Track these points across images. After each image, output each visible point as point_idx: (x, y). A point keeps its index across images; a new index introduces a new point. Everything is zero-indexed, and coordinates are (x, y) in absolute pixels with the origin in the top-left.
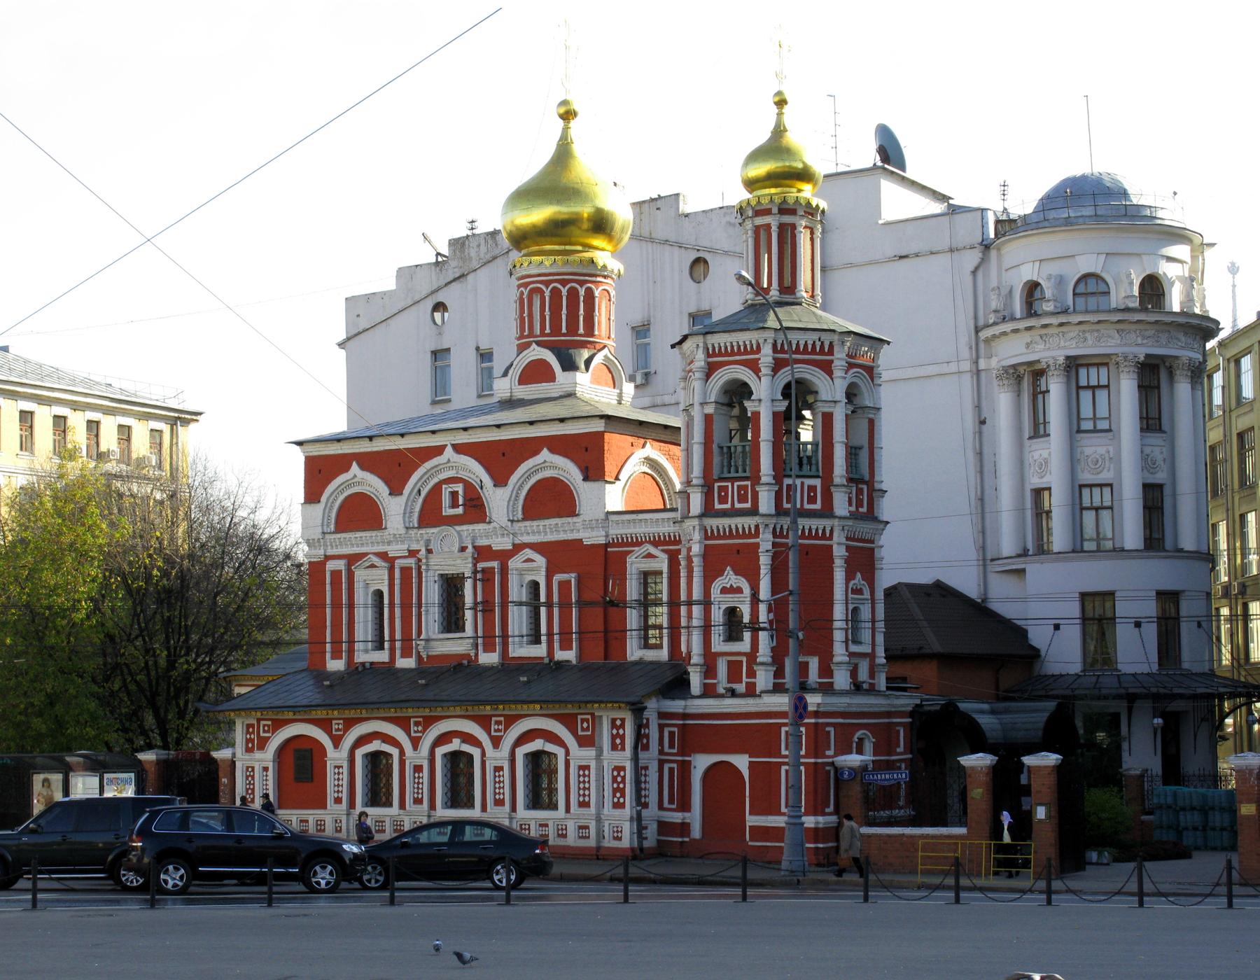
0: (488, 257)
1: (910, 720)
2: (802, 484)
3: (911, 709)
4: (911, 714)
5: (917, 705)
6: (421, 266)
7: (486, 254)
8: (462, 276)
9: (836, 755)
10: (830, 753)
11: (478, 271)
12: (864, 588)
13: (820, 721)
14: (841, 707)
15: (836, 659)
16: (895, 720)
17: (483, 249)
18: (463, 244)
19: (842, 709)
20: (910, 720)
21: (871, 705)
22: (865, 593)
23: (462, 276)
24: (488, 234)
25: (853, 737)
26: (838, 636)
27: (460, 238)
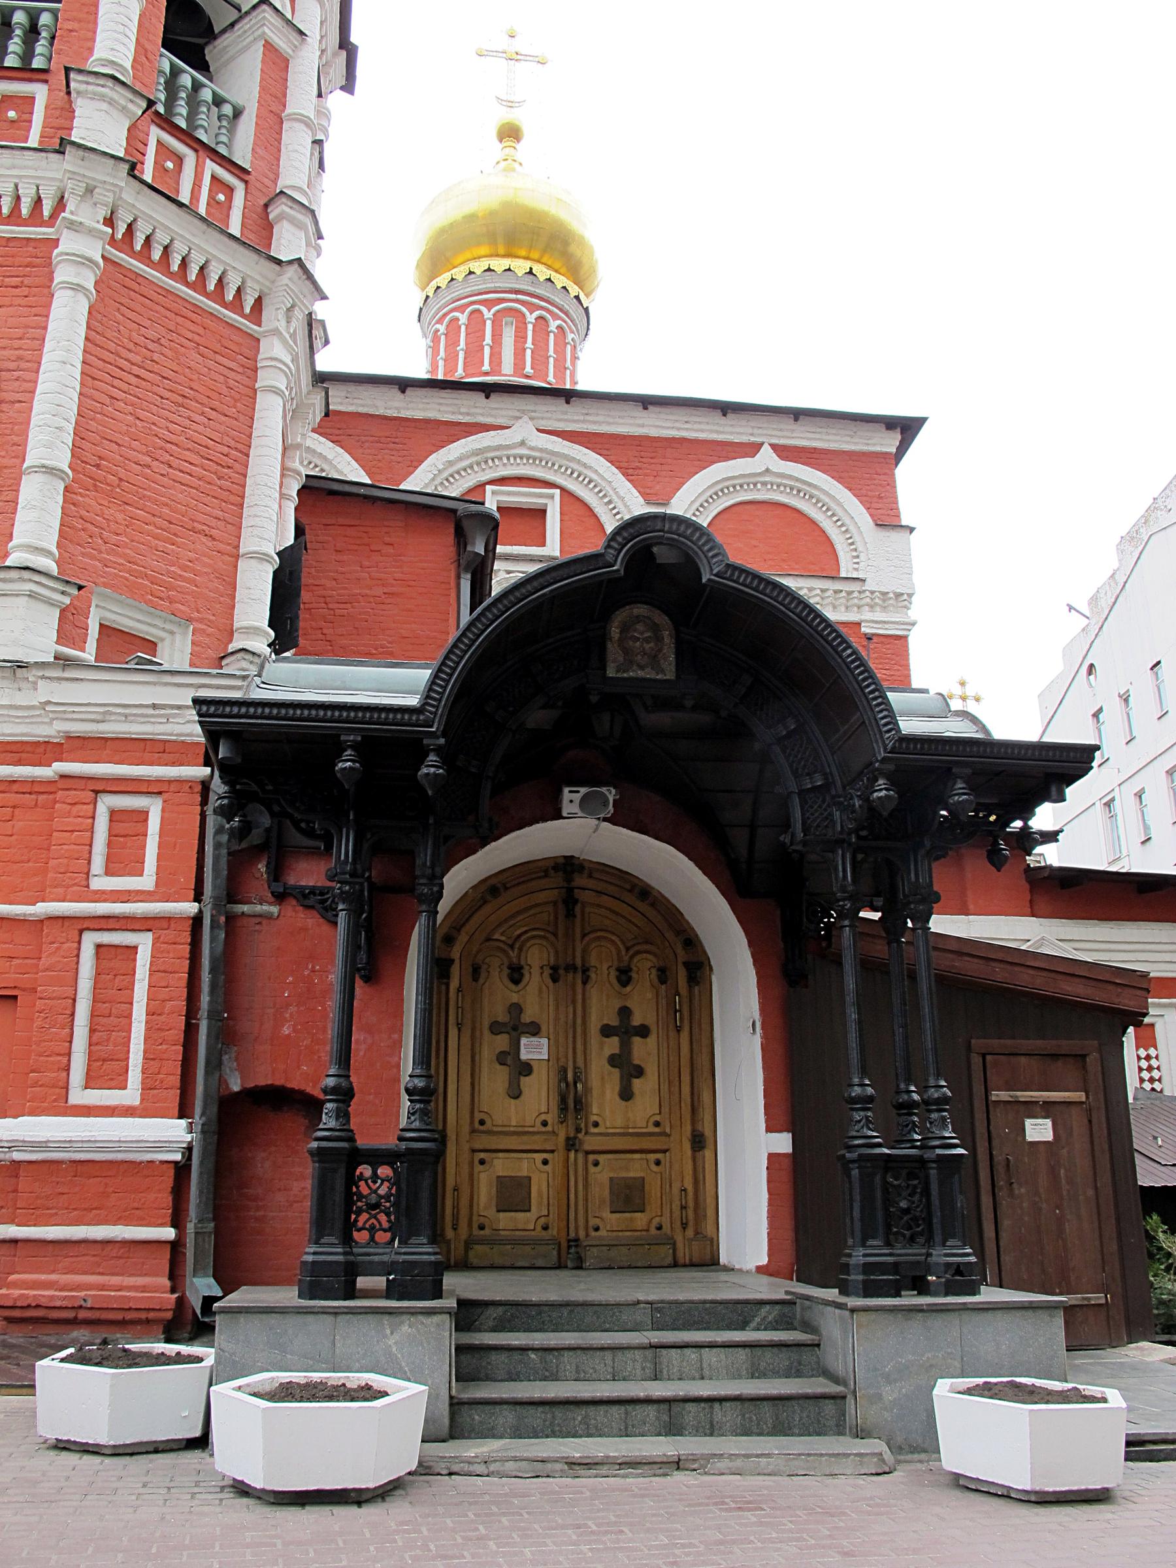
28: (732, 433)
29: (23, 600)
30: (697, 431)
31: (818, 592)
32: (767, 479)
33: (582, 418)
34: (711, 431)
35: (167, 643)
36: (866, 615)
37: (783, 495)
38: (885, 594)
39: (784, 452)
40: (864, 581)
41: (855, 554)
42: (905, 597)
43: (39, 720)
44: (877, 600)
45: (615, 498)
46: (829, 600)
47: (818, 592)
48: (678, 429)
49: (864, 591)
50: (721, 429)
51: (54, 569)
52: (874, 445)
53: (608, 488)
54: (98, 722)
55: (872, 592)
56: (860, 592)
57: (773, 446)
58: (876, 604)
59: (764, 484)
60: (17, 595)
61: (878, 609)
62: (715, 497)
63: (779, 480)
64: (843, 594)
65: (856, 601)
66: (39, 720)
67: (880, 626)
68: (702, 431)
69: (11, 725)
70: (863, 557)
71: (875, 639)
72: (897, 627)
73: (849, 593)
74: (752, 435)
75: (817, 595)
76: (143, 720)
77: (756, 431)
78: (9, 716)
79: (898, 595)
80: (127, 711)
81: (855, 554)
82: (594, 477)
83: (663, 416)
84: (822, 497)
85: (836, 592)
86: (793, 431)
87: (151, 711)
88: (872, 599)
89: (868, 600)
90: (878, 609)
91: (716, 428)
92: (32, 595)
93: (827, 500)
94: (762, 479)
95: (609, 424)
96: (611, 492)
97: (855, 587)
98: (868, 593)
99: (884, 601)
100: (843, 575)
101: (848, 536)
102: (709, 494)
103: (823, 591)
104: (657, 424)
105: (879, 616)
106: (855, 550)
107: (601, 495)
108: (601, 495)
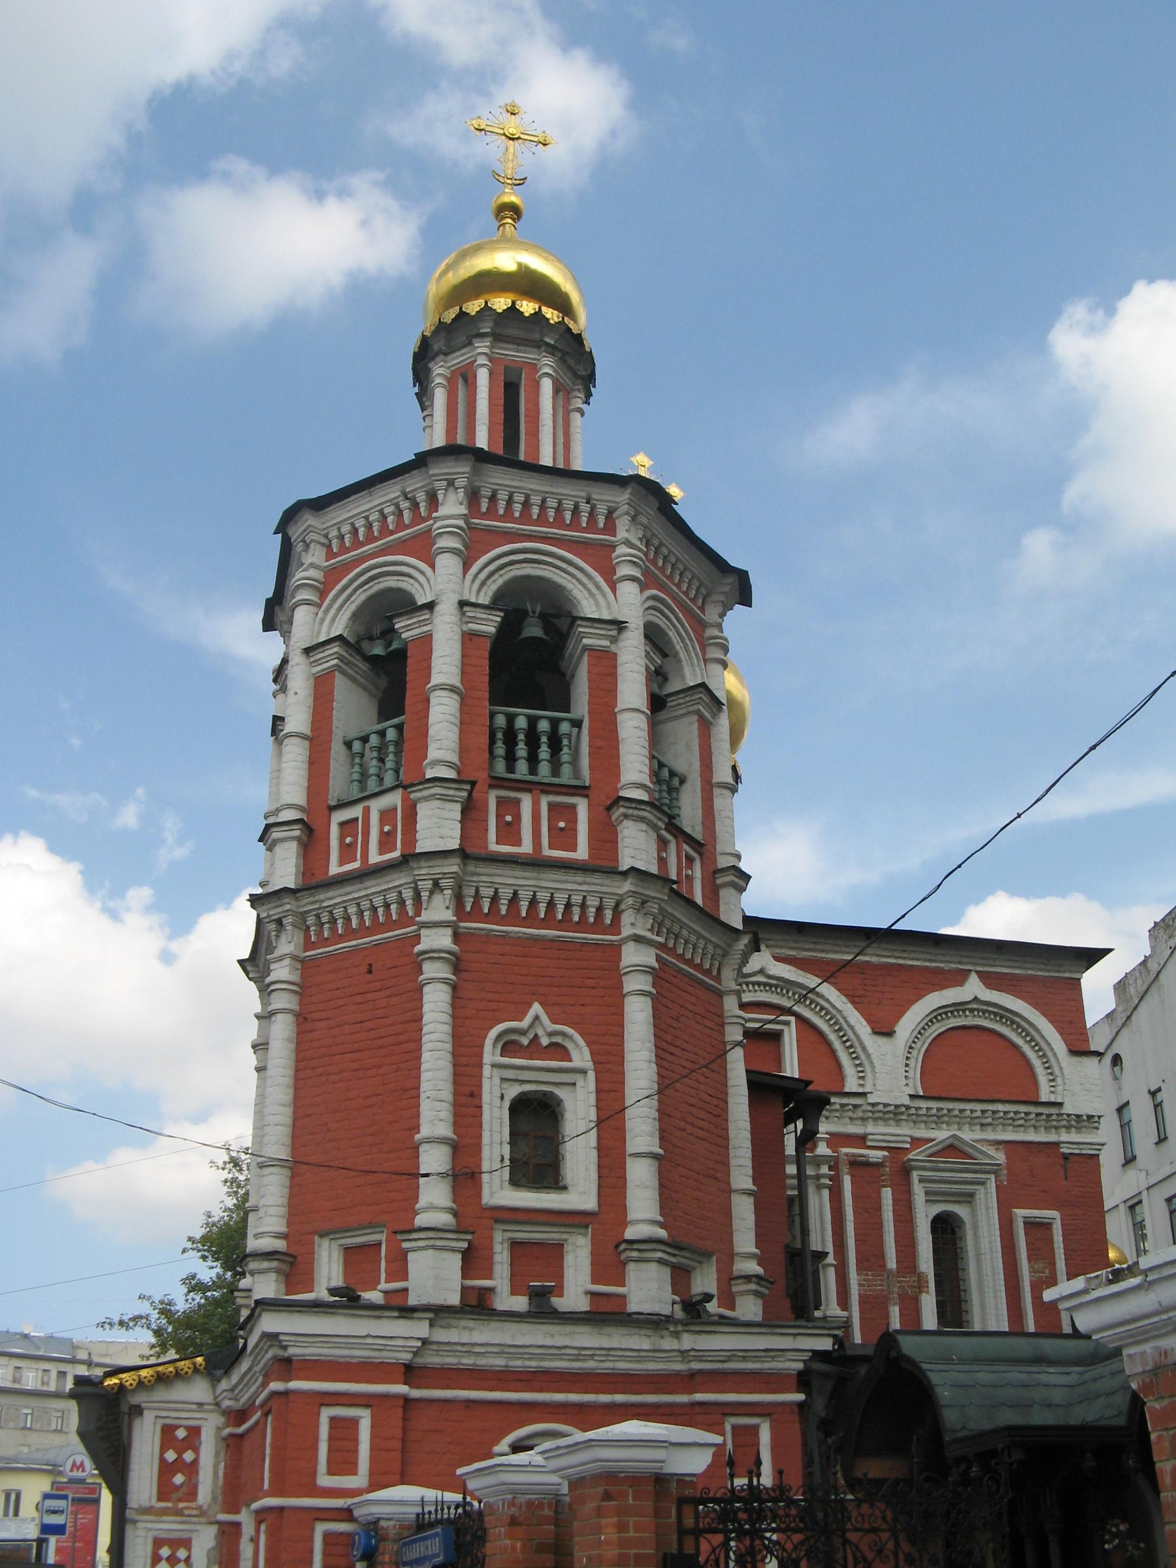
0: (1144, 988)
1: (801, 1397)
2: (367, 811)
3: (800, 1366)
4: (803, 1380)
5: (817, 1355)
6: (1097, 1023)
7: (1142, 986)
8: (1129, 1018)
9: (376, 1484)
10: (360, 1480)
11: (1139, 1008)
12: (569, 1045)
13: (294, 1385)
14: (397, 1349)
15: (421, 1220)
16: (699, 1397)
17: (1139, 981)
18: (1125, 984)
19: (406, 1357)
20: (801, 1397)
21: (581, 1353)
22: (574, 1054)
23: (1129, 1018)
24: (1140, 964)
25: (497, 1441)
26: (433, 1159)
27: (1120, 981)
28: (942, 962)
29: (653, 1266)
30: (912, 959)
31: (1023, 1115)
32: (975, 1006)
33: (812, 946)
34: (925, 960)
35: (698, 1271)
36: (1064, 1137)
37: (988, 1021)
38: (1078, 1116)
39: (989, 980)
40: (1060, 1105)
41: (1051, 1077)
42: (1096, 1119)
43: (676, 1359)
44: (1073, 1123)
45: (845, 1026)
46: (1033, 1122)
47: (1023, 1115)
48: (896, 958)
49: (1062, 1114)
50: (934, 958)
51: (662, 1233)
52: (1065, 972)
53: (839, 1017)
54: (723, 1362)
55: (1069, 1115)
56: (1057, 1115)
57: (977, 972)
58: (1072, 1126)
59: (972, 1010)
60: (649, 1261)
61: (1073, 1130)
62: (930, 1024)
63: (985, 1008)
64: (1044, 1117)
65: (1054, 1123)
66: (676, 1359)
67: (1075, 1146)
68: (917, 959)
69: (652, 1363)
70: (1059, 1081)
71: (1072, 1159)
72: (1090, 1147)
73: (1049, 1116)
74: (960, 963)
75: (1022, 1118)
76: (755, 1359)
77: (964, 960)
78: (654, 1357)
79: (1090, 1117)
80: (747, 1354)
81: (1051, 1077)
82: (826, 1005)
83: (883, 946)
84: (1023, 1023)
85: (1038, 1115)
86: (995, 960)
87: (763, 1354)
88: (1068, 1121)
89: (1065, 1123)
90: (1073, 1130)
91: (929, 957)
92: (660, 1261)
93: (1026, 1026)
94: (969, 1006)
95: (835, 952)
96: (842, 1021)
97: (1053, 1111)
98: (1065, 1117)
99: (1078, 1122)
100: (1043, 1100)
101: (1045, 1060)
102: (925, 1021)
103: (1027, 1114)
104: (879, 953)
105: (1074, 1137)
106: (1051, 1074)
107: (832, 1022)
108: (832, 1022)
